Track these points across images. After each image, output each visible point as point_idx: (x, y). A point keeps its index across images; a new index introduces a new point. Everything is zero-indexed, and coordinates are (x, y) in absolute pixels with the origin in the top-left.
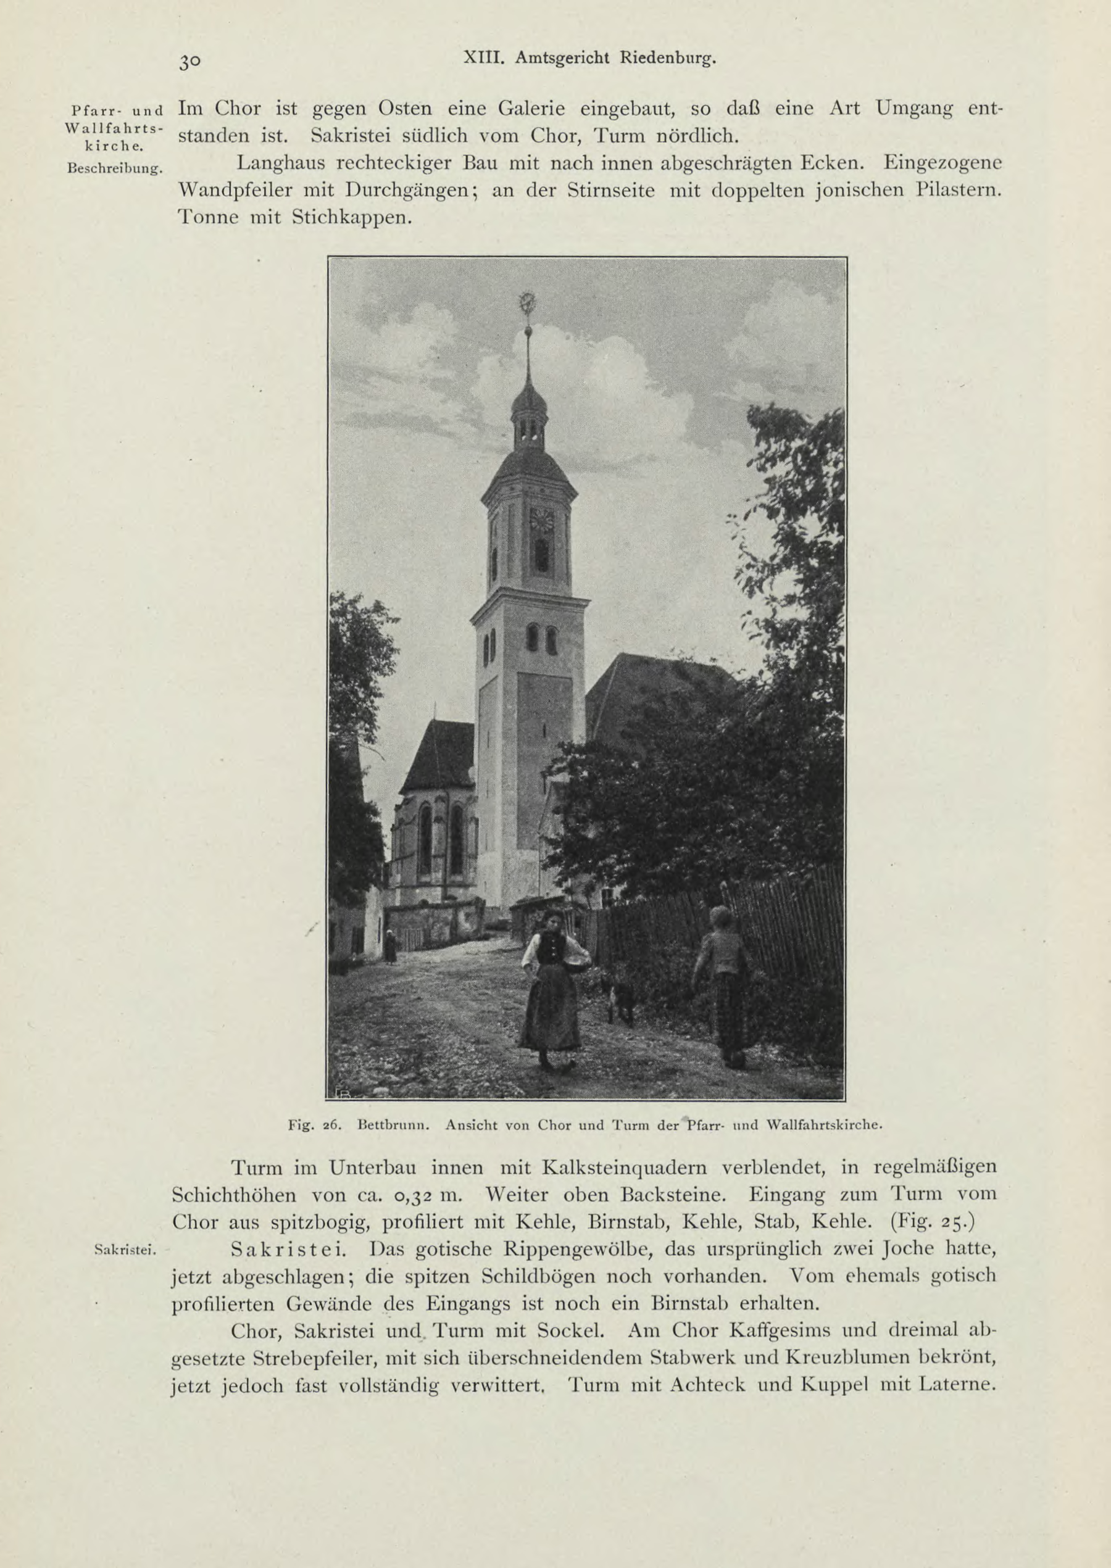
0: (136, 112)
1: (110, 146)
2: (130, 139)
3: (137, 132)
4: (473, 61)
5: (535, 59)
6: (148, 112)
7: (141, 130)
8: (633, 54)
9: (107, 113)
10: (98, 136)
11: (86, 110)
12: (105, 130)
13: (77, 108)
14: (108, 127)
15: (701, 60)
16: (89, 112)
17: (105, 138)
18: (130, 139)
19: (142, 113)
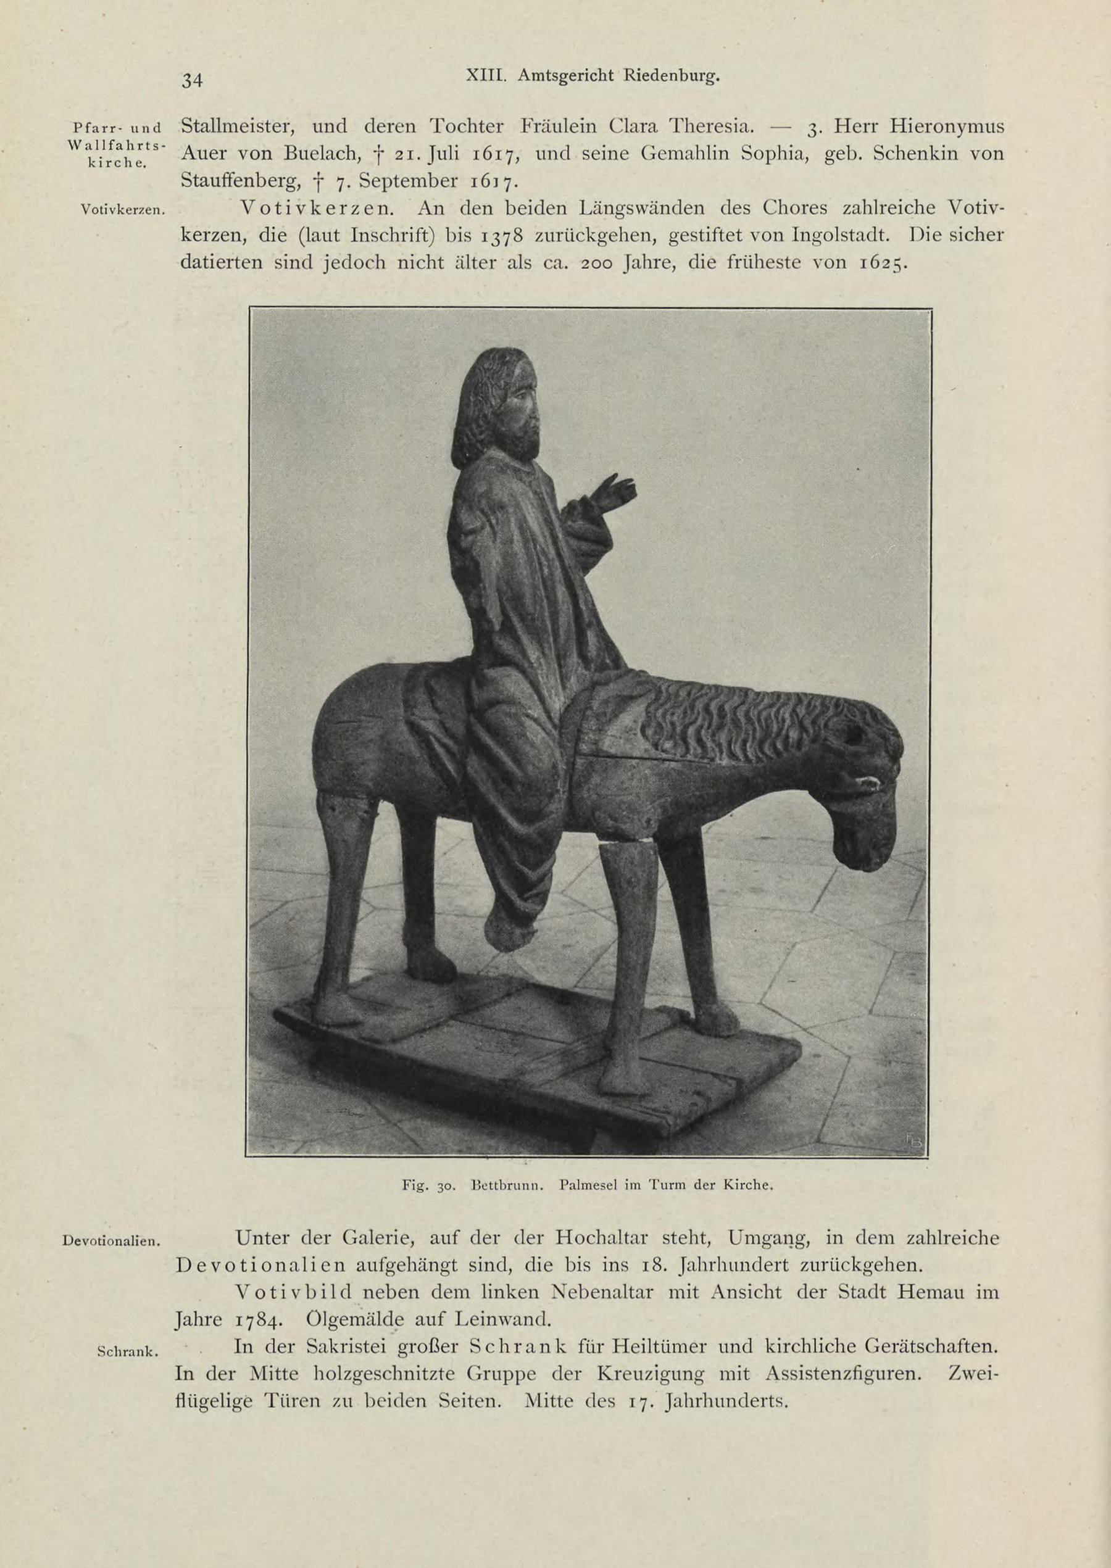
0: (135, 130)
1: (113, 163)
2: (133, 156)
3: (140, 149)
4: (476, 79)
5: (537, 77)
6: (146, 129)
7: (144, 147)
8: (636, 71)
9: (108, 130)
10: (100, 152)
11: (87, 127)
12: (107, 146)
13: (78, 125)
14: (111, 144)
15: (704, 77)
16: (90, 129)
17: (108, 155)
18: (133, 156)
19: (140, 129)
